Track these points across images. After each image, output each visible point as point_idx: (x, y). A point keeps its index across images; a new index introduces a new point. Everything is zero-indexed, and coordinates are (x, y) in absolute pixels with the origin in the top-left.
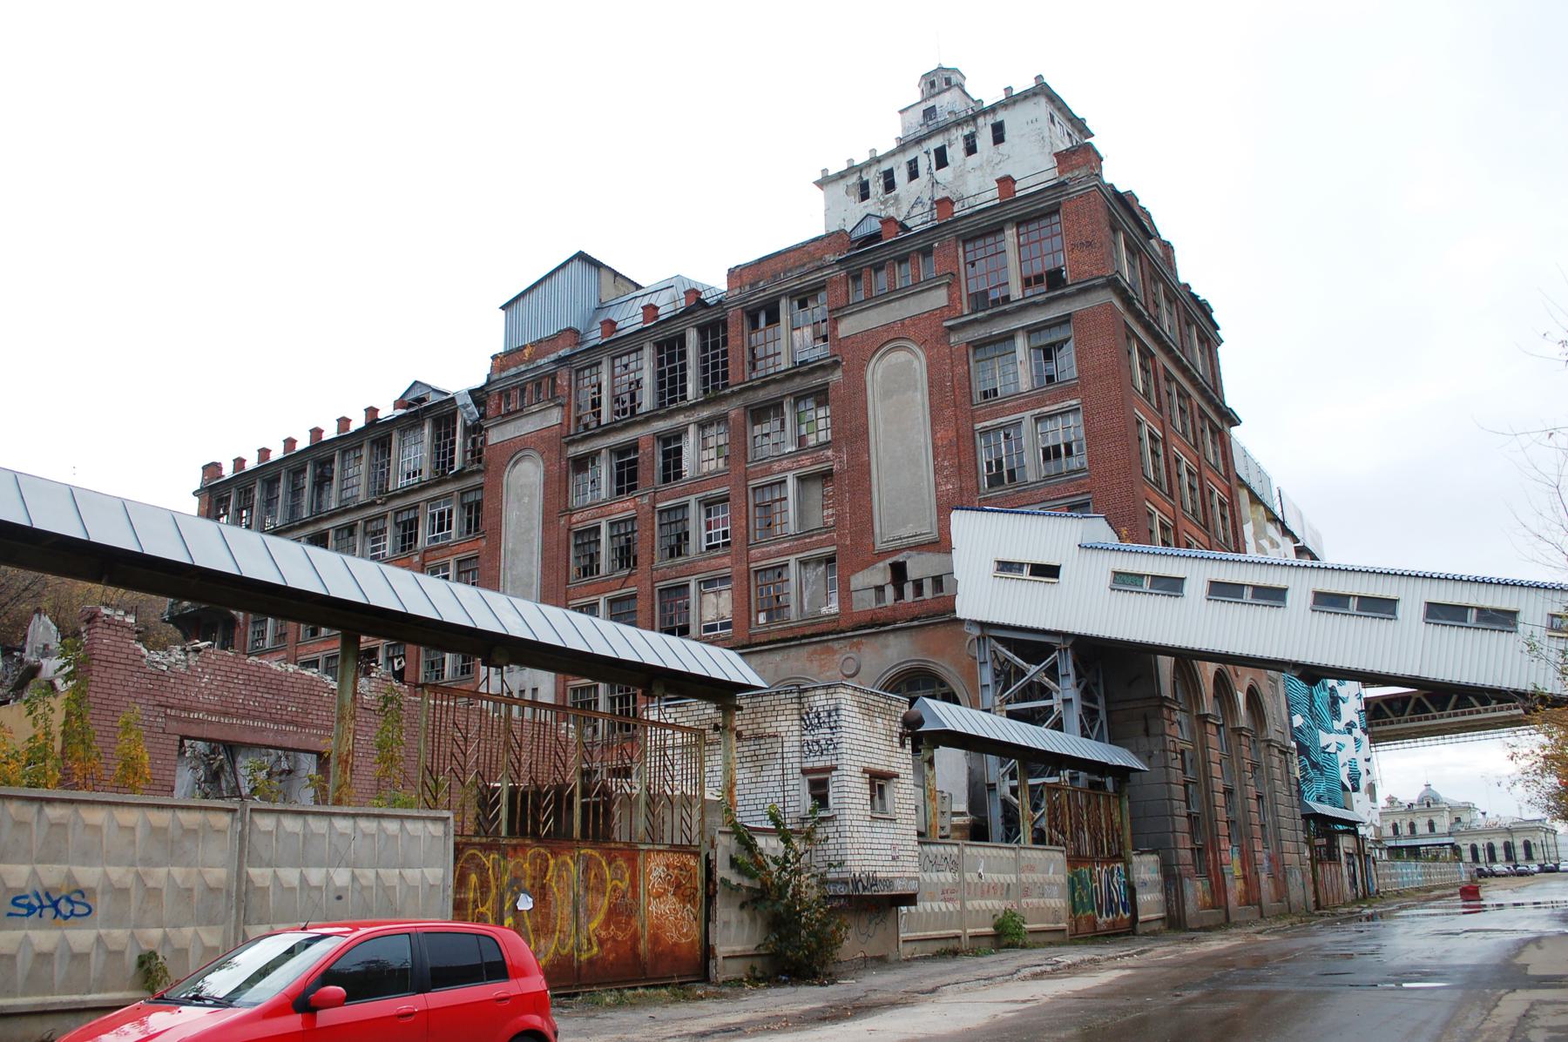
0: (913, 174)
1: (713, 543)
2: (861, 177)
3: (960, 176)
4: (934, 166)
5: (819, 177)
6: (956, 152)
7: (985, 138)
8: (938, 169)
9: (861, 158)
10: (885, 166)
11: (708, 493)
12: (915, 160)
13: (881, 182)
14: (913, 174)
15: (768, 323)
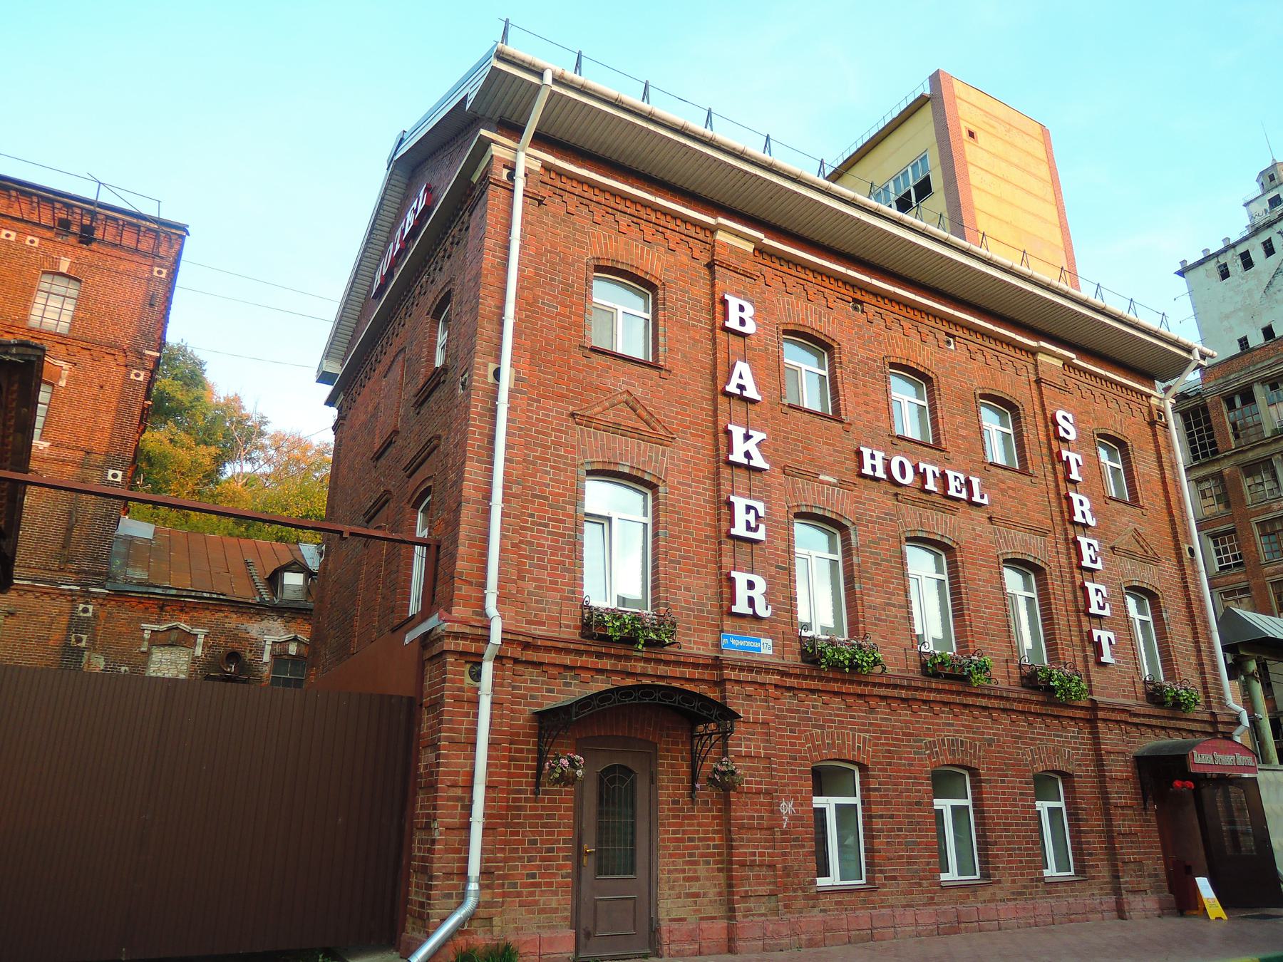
1: (1225, 564)
2: (1218, 262)
5: (1179, 268)
10: (1241, 249)
11: (1215, 529)
12: (1270, 240)
15: (1244, 404)
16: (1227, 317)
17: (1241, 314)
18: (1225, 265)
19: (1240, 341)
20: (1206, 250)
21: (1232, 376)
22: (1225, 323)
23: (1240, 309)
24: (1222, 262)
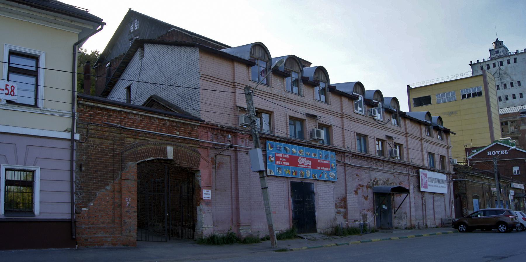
0: (494, 66)
3: (506, 68)
4: (500, 65)
6: (505, 63)
7: (512, 61)
8: (501, 66)
10: (487, 63)
12: (495, 63)
13: (486, 67)
14: (494, 66)
15: (505, 124)
18: (483, 66)
21: (504, 118)
24: (482, 65)
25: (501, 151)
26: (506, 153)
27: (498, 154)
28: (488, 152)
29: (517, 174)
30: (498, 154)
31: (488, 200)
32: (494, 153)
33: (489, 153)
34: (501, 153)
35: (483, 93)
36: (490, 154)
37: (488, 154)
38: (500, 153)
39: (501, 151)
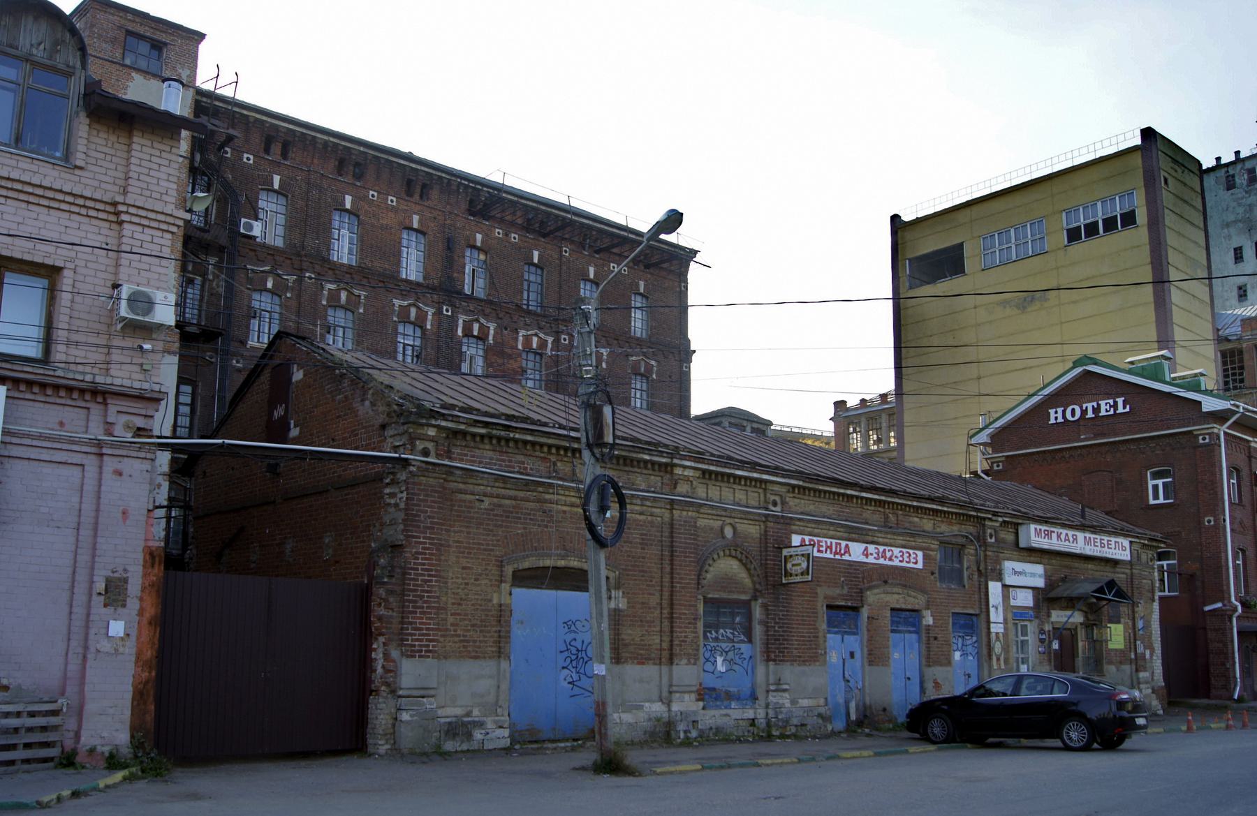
2: (1228, 172)
9: (1228, 158)
10: (1248, 165)
16: (1228, 225)
17: (1241, 225)
18: (1233, 176)
19: (1235, 250)
20: (1218, 159)
22: (1226, 231)
23: (1240, 221)
24: (1231, 172)
25: (1102, 403)
26: (1120, 410)
27: (1090, 415)
28: (1052, 411)
29: (1161, 501)
30: (1090, 415)
31: (747, 604)
32: (1073, 411)
33: (1055, 415)
34: (1103, 413)
35: (1142, 217)
36: (1060, 420)
37: (1052, 421)
38: (1096, 410)
39: (1102, 403)
